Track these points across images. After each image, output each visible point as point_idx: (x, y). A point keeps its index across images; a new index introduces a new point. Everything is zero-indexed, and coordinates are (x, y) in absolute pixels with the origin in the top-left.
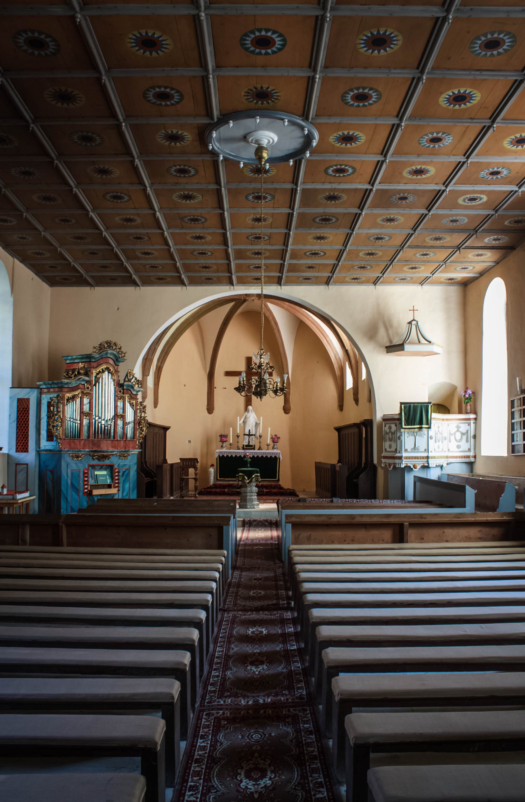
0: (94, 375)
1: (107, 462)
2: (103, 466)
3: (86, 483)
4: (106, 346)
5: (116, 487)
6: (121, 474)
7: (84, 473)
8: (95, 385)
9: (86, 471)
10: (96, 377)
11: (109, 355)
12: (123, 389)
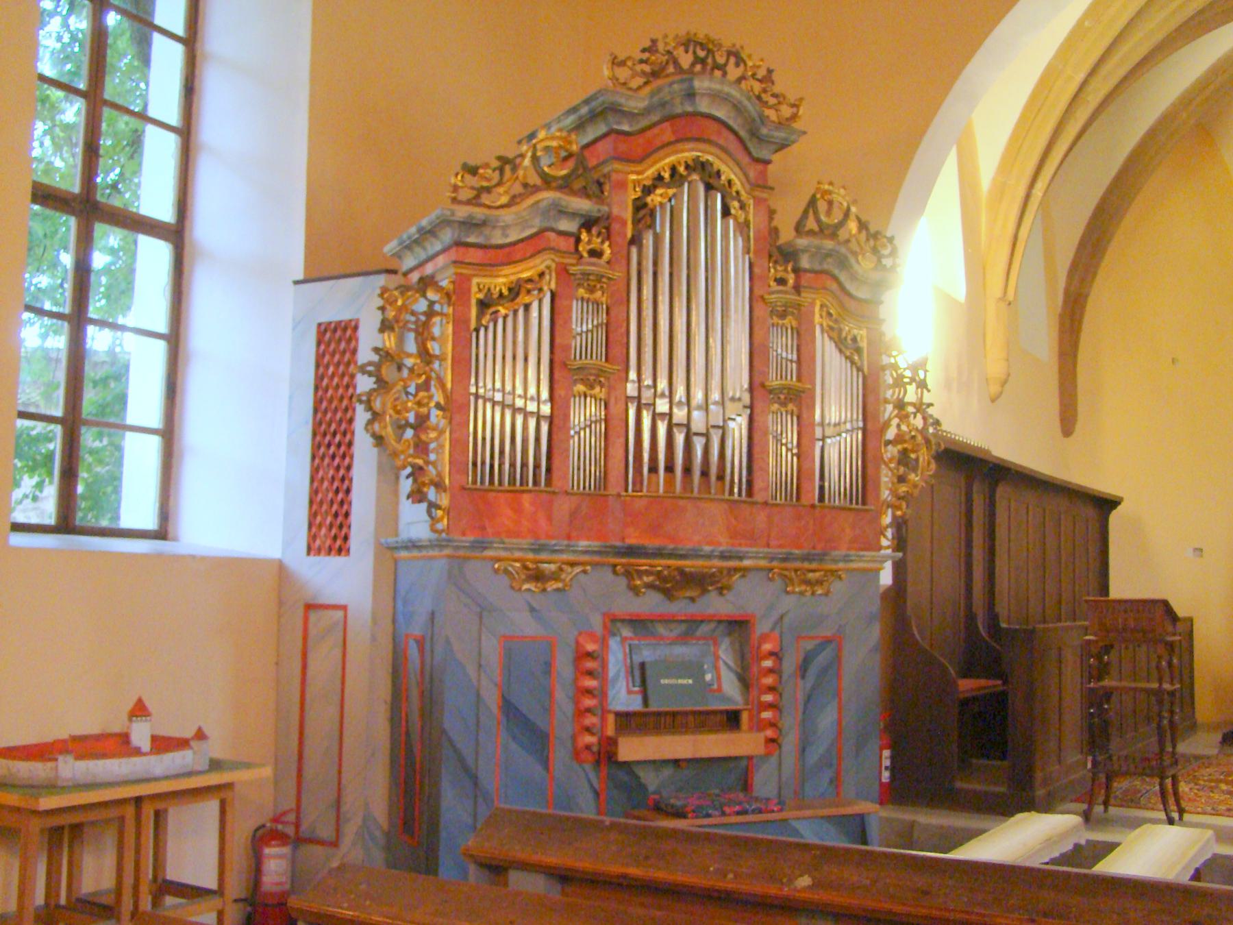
0: (633, 194)
1: (715, 605)
2: (694, 622)
3: (588, 702)
4: (686, 60)
5: (760, 726)
6: (790, 664)
7: (582, 655)
8: (636, 240)
9: (590, 647)
10: (640, 205)
11: (704, 106)
12: (796, 271)
